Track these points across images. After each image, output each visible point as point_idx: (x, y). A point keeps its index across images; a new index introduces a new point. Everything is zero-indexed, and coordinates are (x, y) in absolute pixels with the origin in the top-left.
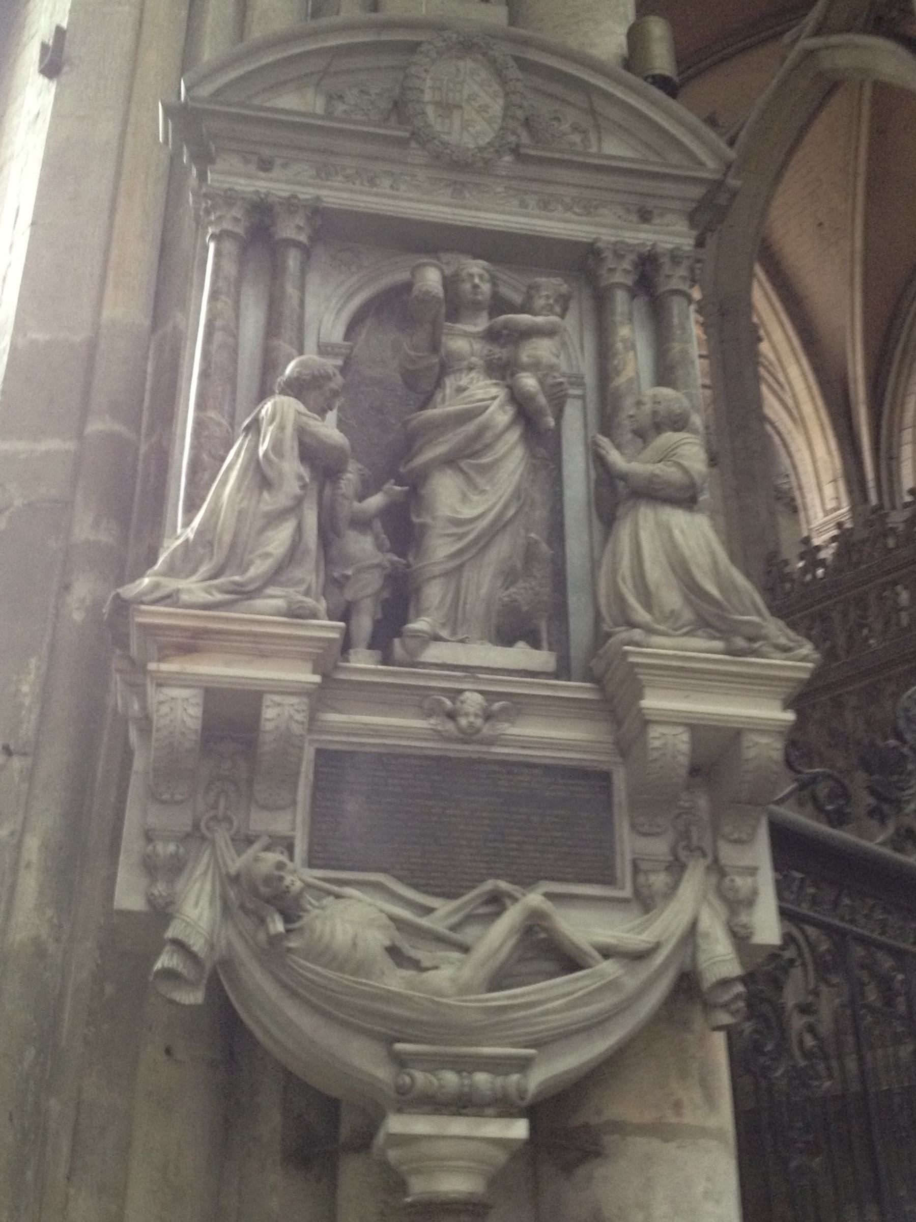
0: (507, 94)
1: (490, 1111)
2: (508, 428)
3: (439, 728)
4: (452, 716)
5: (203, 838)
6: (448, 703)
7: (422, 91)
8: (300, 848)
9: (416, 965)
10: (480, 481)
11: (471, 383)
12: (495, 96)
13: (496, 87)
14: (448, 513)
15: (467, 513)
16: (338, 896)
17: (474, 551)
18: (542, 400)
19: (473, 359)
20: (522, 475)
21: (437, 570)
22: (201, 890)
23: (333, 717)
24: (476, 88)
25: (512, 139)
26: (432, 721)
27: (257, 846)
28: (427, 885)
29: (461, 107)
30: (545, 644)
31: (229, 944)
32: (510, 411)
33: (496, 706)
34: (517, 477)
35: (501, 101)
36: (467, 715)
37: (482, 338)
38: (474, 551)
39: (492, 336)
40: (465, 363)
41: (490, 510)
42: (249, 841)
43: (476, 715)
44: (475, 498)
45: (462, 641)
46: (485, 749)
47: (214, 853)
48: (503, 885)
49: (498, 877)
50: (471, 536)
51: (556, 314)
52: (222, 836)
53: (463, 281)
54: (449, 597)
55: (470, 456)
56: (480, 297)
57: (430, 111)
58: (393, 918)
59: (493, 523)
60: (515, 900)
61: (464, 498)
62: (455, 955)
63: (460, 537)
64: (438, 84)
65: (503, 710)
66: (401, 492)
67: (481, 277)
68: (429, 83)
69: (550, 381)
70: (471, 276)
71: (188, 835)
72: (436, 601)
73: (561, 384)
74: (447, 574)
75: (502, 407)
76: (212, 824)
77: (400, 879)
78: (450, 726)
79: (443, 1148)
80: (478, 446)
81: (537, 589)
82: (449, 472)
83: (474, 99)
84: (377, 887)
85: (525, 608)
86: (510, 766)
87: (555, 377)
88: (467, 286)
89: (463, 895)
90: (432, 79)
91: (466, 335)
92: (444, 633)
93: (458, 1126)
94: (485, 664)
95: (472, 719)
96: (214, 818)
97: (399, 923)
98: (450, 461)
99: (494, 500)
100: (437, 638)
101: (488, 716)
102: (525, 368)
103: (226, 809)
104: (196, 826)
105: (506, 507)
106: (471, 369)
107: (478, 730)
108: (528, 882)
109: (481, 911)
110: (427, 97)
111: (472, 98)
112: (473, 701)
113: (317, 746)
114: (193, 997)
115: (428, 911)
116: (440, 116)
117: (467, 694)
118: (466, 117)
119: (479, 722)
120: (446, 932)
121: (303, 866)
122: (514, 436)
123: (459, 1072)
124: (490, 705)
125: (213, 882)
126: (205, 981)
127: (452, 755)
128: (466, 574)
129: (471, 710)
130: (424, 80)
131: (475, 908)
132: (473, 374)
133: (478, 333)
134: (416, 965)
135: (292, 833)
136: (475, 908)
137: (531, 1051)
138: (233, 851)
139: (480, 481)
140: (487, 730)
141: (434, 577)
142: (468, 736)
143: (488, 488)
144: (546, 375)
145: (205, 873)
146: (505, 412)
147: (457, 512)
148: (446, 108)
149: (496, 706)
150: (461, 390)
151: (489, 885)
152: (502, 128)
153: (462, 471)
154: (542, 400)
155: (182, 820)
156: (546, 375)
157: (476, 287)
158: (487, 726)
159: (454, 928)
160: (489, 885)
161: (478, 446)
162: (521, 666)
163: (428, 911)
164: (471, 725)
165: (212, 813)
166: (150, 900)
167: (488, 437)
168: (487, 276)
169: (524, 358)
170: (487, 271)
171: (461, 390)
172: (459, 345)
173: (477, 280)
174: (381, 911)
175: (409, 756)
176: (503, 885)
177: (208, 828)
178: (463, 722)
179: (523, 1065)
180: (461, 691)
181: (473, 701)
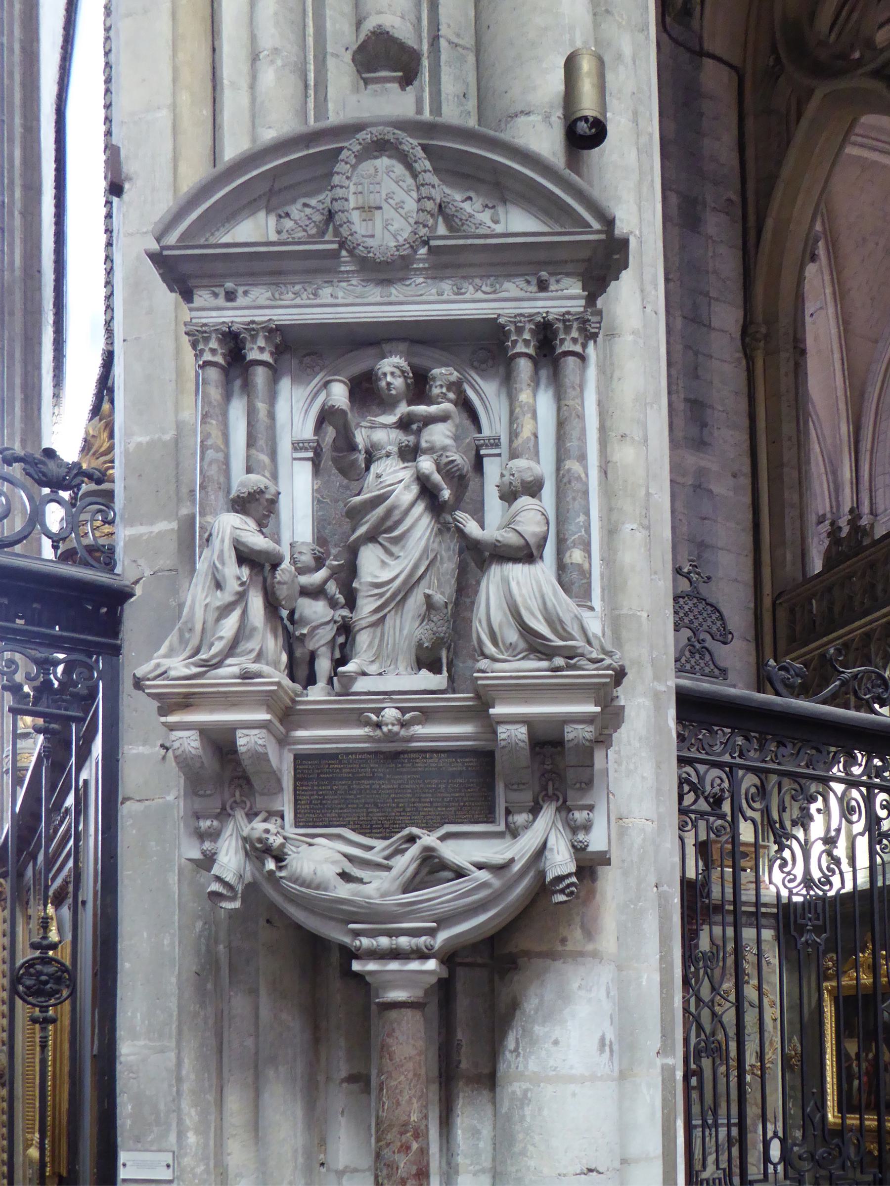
0: (418, 189)
1: (412, 956)
2: (413, 505)
3: (371, 734)
4: (378, 725)
5: (230, 815)
6: (374, 717)
7: (347, 200)
8: (289, 816)
9: (360, 881)
10: (394, 549)
11: (384, 470)
12: (408, 192)
13: (410, 181)
14: (370, 579)
15: (385, 576)
16: (311, 845)
17: (392, 605)
18: (437, 478)
19: (389, 448)
20: (429, 539)
21: (364, 623)
22: (229, 844)
23: (300, 733)
24: (394, 187)
25: (423, 231)
26: (367, 729)
27: (259, 818)
28: (371, 833)
29: (380, 208)
30: (445, 669)
31: (253, 875)
32: (415, 489)
33: (408, 716)
34: (423, 543)
35: (415, 195)
36: (387, 725)
37: (396, 428)
38: (392, 605)
39: (404, 424)
40: (384, 452)
41: (401, 572)
42: (256, 814)
43: (393, 725)
44: (392, 563)
45: (380, 674)
46: (405, 745)
47: (235, 822)
48: (415, 831)
49: (413, 824)
50: (388, 595)
51: (450, 401)
52: (240, 815)
53: (380, 380)
54: (377, 641)
55: (385, 532)
56: (393, 392)
57: (355, 216)
58: (346, 856)
59: (405, 582)
60: (420, 838)
61: (383, 563)
62: (385, 874)
63: (381, 595)
64: (360, 188)
65: (412, 718)
66: (339, 565)
67: (392, 374)
68: (352, 188)
69: (444, 460)
70: (385, 374)
71: (219, 814)
72: (365, 647)
73: (453, 461)
74: (374, 625)
75: (407, 487)
76: (234, 805)
77: (354, 830)
78: (378, 733)
79: (388, 977)
80: (389, 523)
81: (435, 629)
82: (371, 546)
83: (391, 198)
84: (339, 837)
85: (426, 645)
86: (422, 752)
87: (447, 457)
88: (383, 384)
89: (392, 837)
90: (354, 184)
91: (385, 426)
92: (373, 669)
93: (394, 966)
94: (397, 689)
95: (390, 727)
96: (235, 802)
97: (350, 858)
98: (371, 537)
99: (406, 562)
100: (364, 674)
101: (403, 724)
102: (425, 452)
103: (241, 796)
104: (223, 808)
105: (416, 567)
106: (388, 455)
107: (397, 734)
108: (431, 828)
109: (404, 846)
110: (352, 204)
111: (389, 197)
112: (390, 713)
113: (295, 752)
114: (236, 904)
115: (371, 848)
116: (364, 220)
117: (386, 710)
118: (385, 217)
119: (396, 728)
120: (381, 860)
121: (291, 826)
122: (420, 508)
123: (391, 937)
124: (403, 715)
125: (237, 840)
126: (240, 895)
127: (384, 750)
128: (389, 621)
129: (389, 721)
130: (348, 188)
131: (400, 845)
132: (389, 461)
133: (395, 423)
134: (360, 881)
135: (282, 808)
136: (400, 845)
137: (434, 924)
138: (246, 820)
139: (394, 549)
140: (403, 732)
141: (362, 629)
142: (391, 737)
143: (401, 554)
144: (441, 455)
145: (231, 835)
146: (410, 491)
147: (376, 577)
148: (369, 210)
149: (408, 716)
150: (379, 476)
151: (406, 832)
152: (416, 223)
153: (381, 544)
154: (437, 478)
155: (215, 805)
156: (441, 455)
157: (389, 384)
158: (403, 729)
159: (387, 858)
160: (406, 832)
161: (389, 523)
162: (422, 688)
163: (371, 848)
164: (390, 731)
165: (232, 800)
166: (203, 853)
167: (396, 515)
168: (398, 372)
169: (424, 445)
170: (398, 367)
171: (379, 476)
172: (380, 436)
173: (389, 378)
174: (339, 852)
175: (356, 753)
176: (415, 831)
177: (231, 809)
178: (385, 729)
179: (432, 932)
180: (384, 708)
181: (390, 713)
